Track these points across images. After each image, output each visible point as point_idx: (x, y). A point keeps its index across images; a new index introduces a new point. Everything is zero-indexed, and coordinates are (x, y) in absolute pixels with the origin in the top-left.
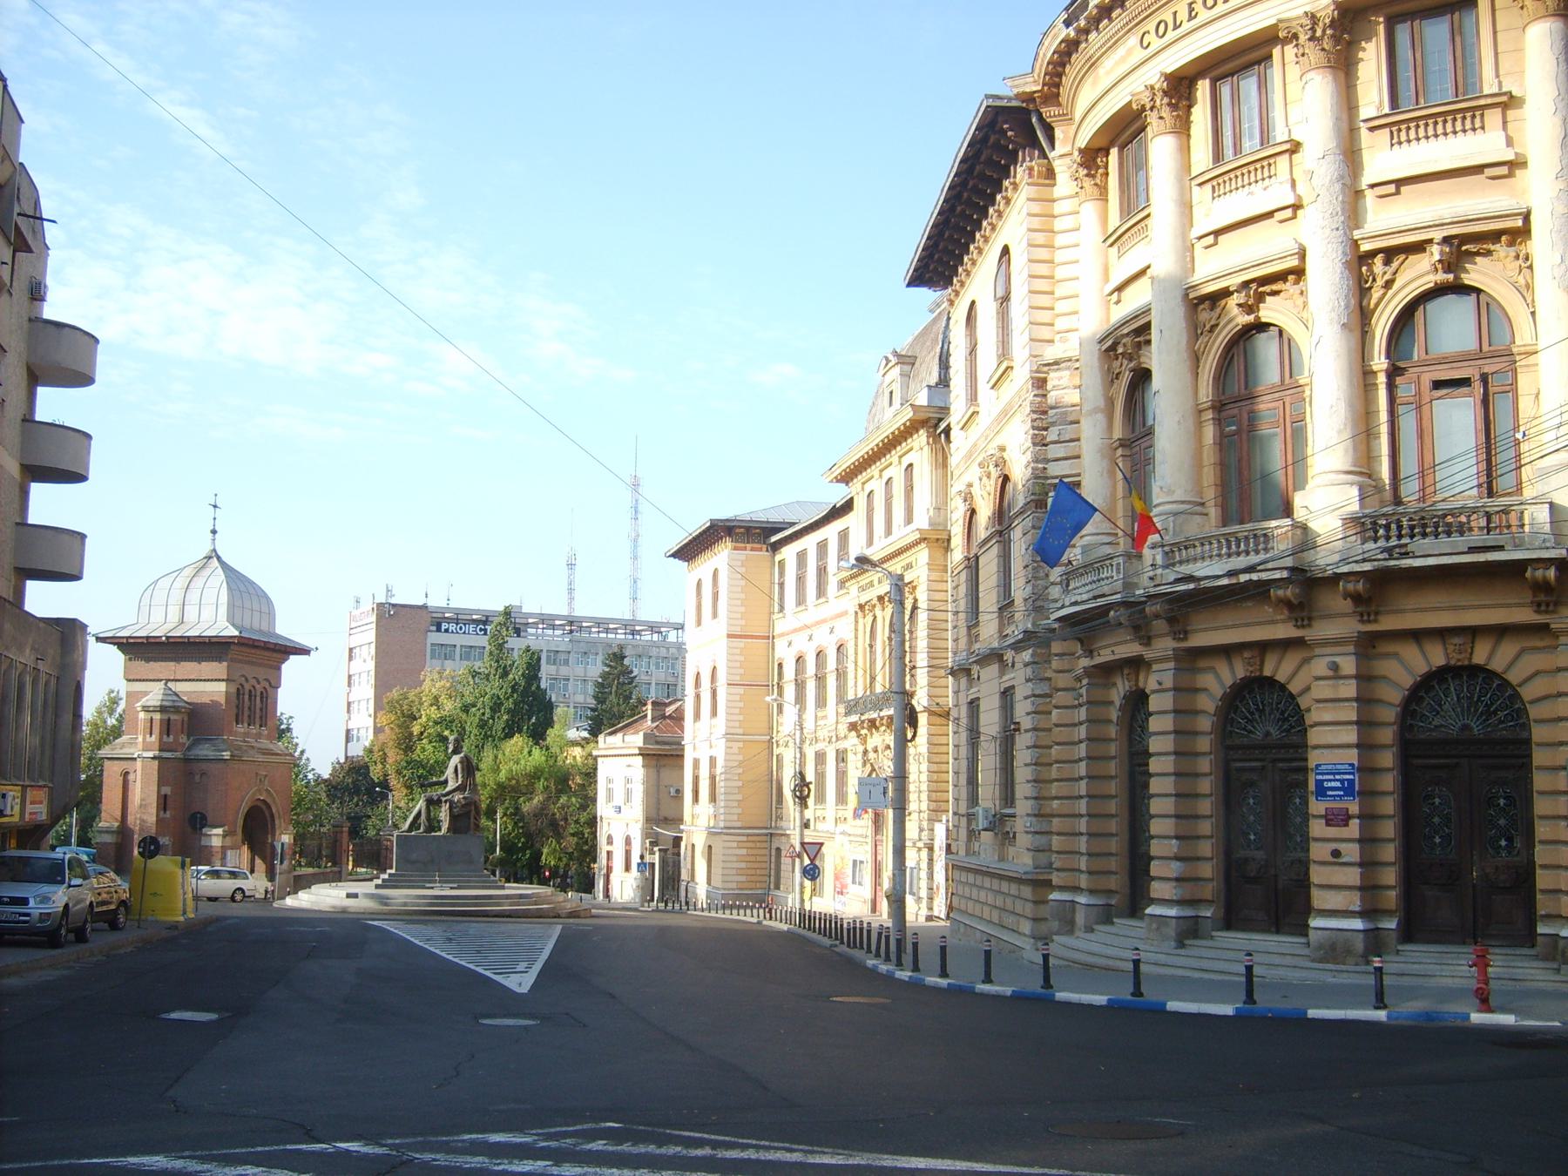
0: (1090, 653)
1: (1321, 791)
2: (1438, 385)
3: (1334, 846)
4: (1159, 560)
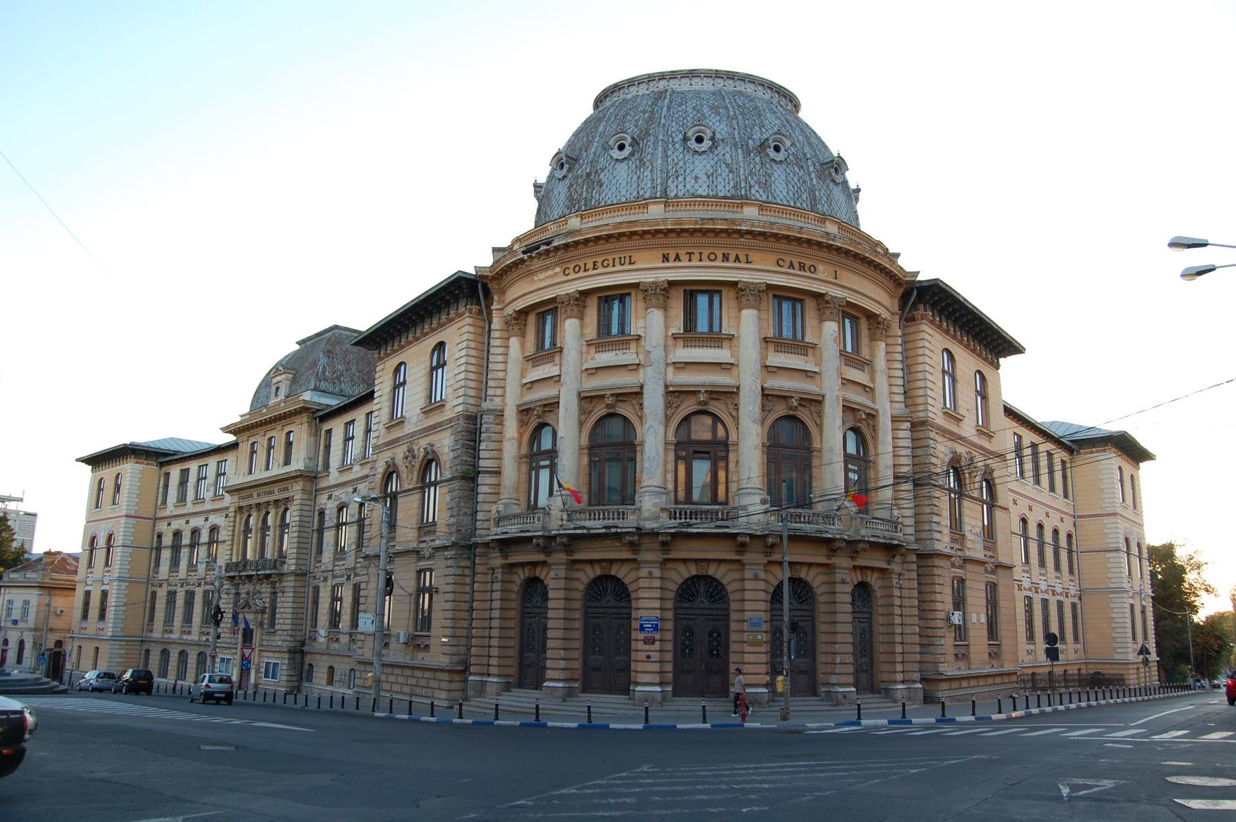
0: (506, 557)
1: (642, 628)
2: (695, 452)
4: (565, 517)
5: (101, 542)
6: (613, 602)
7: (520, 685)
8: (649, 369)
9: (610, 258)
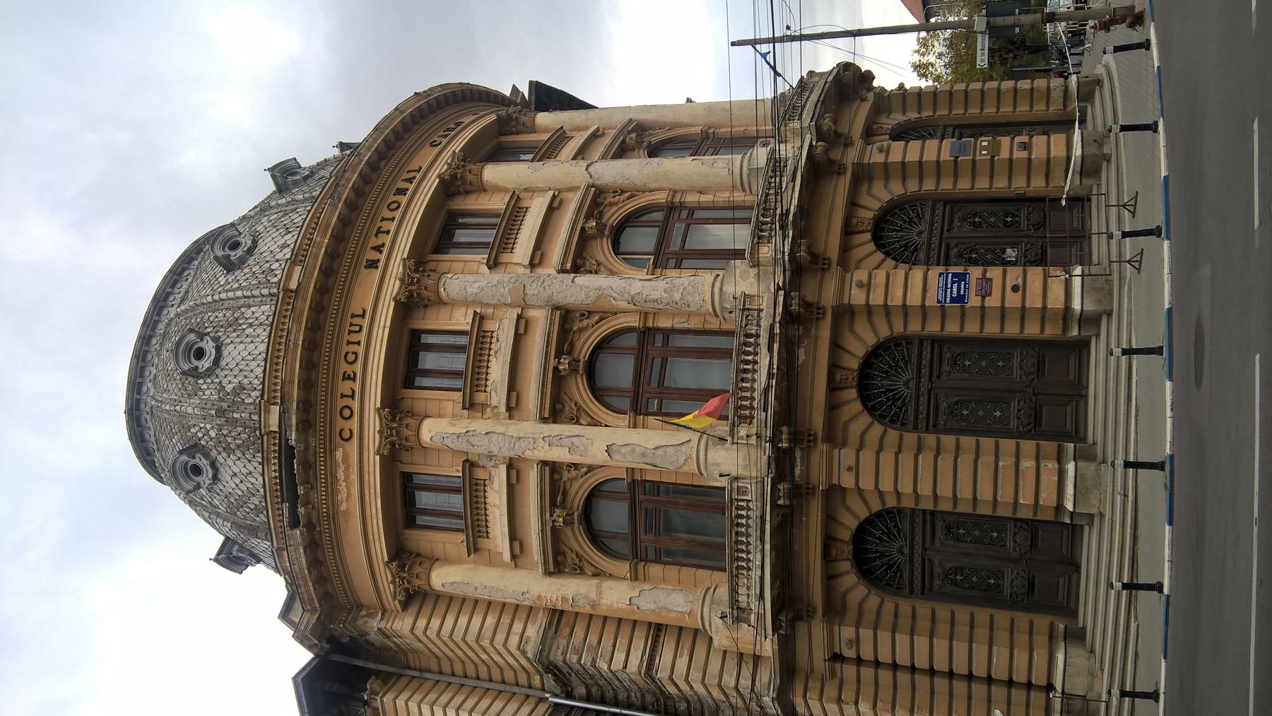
0: (810, 614)
3: (1008, 289)
6: (909, 374)
7: (1070, 611)
8: (529, 291)
9: (346, 348)
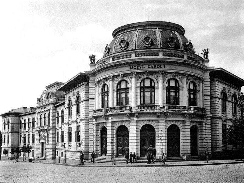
5: (6, 123)
